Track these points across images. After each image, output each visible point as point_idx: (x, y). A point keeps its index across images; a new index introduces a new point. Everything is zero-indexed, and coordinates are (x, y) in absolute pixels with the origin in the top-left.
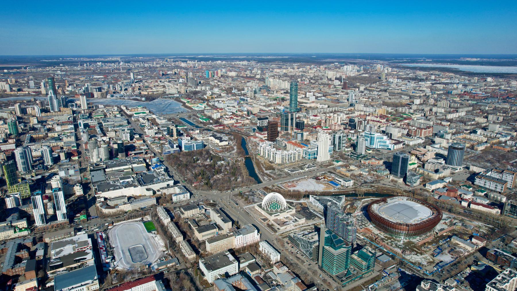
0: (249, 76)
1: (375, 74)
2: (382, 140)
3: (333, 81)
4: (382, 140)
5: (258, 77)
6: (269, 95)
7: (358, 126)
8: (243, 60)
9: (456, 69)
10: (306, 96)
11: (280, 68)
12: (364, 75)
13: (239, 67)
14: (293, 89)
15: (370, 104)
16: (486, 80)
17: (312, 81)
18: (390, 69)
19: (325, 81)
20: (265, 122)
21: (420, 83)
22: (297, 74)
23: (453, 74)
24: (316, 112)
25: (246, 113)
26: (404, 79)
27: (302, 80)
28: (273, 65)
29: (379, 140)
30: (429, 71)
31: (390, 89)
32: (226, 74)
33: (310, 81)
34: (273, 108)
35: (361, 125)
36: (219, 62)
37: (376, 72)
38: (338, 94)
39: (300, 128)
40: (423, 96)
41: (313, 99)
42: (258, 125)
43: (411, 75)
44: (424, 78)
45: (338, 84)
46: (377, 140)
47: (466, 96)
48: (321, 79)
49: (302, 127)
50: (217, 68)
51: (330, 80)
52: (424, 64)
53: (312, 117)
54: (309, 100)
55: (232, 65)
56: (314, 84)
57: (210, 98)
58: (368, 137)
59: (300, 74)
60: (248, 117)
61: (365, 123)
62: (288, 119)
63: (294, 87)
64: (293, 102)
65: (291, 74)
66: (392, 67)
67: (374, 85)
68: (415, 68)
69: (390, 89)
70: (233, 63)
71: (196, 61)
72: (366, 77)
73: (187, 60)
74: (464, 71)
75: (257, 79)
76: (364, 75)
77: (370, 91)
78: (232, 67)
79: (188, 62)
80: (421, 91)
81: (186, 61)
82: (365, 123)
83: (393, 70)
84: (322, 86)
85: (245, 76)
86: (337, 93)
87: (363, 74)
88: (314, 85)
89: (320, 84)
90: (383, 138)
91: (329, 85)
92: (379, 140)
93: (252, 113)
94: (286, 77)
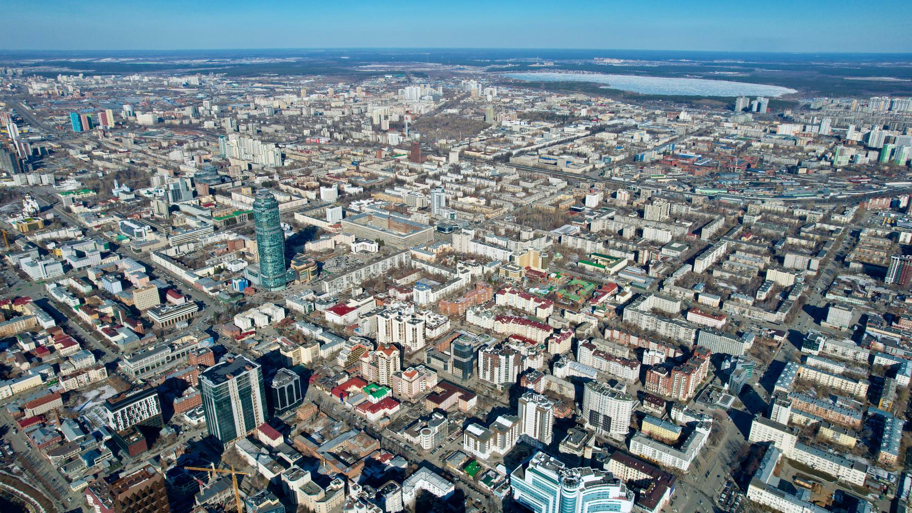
0: (186, 122)
1: (472, 105)
2: (604, 501)
3: (385, 132)
4: (604, 501)
5: (209, 125)
6: (220, 199)
8: (191, 70)
9: (605, 85)
10: (318, 196)
11: (270, 93)
12: (450, 111)
13: (176, 93)
14: (265, 220)
15: (487, 219)
16: (678, 117)
17: (336, 135)
18: (495, 91)
19: (367, 133)
20: (144, 407)
21: (566, 129)
22: (305, 112)
23: (610, 100)
24: (345, 282)
26: (532, 118)
27: (313, 133)
28: (257, 85)
29: (594, 503)
30: (568, 94)
31: (514, 152)
32: (131, 118)
33: (331, 134)
34: (211, 270)
35: (496, 369)
36: (136, 77)
37: (470, 99)
38: (401, 183)
39: (284, 404)
40: (591, 170)
41: (334, 214)
43: (540, 107)
44: (566, 112)
45: (396, 143)
46: (587, 505)
47: (676, 169)
48: (359, 129)
49: (291, 401)
50: (115, 97)
51: (377, 129)
52: (545, 74)
53: (332, 318)
54: (322, 217)
55: (163, 85)
56: (342, 143)
57: (26, 229)
58: (553, 493)
59: (312, 112)
60: (107, 337)
61: (507, 363)
62: (228, 401)
63: (267, 212)
64: (269, 259)
65: (291, 113)
66: (497, 84)
67: (476, 142)
68: (535, 85)
69: (514, 152)
70: (166, 83)
71: (81, 75)
72: (453, 114)
73: (55, 69)
74: (623, 92)
75: (204, 130)
76: (450, 111)
77: (474, 160)
78: (159, 93)
79: (59, 77)
80: (579, 155)
81: (54, 75)
82: (507, 363)
83: (499, 92)
84: (360, 152)
85: (177, 122)
86: (400, 177)
87: (446, 106)
88: (343, 149)
89: (356, 145)
90: (606, 495)
91: (378, 146)
92: (594, 503)
94: (277, 122)
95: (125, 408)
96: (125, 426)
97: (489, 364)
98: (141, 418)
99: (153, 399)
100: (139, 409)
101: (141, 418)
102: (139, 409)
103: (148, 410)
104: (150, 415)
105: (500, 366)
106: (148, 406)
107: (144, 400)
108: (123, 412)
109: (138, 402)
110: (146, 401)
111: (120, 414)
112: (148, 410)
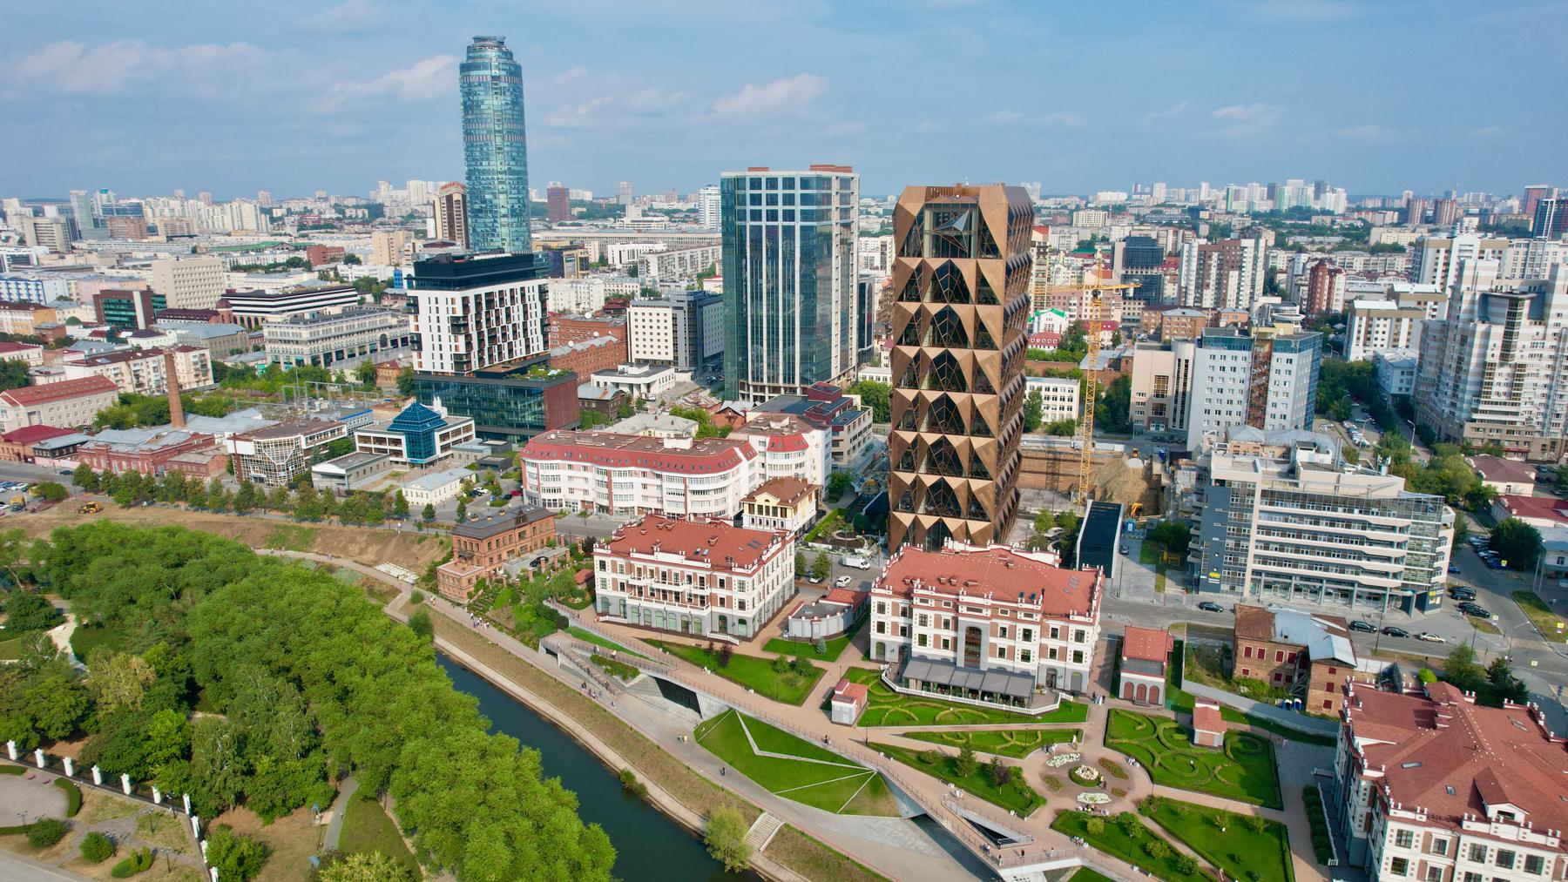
7: (1201, 286)
25: (88, 314)
35: (1234, 274)
42: (438, 355)
93: (156, 306)
95: (482, 291)
96: (481, 359)
97: (1214, 271)
98: (511, 351)
99: (537, 293)
100: (508, 316)
101: (511, 351)
102: (508, 316)
103: (525, 330)
104: (528, 347)
105: (1240, 268)
106: (525, 313)
107: (517, 285)
108: (478, 297)
109: (506, 287)
110: (523, 296)
111: (472, 305)
112: (525, 330)
